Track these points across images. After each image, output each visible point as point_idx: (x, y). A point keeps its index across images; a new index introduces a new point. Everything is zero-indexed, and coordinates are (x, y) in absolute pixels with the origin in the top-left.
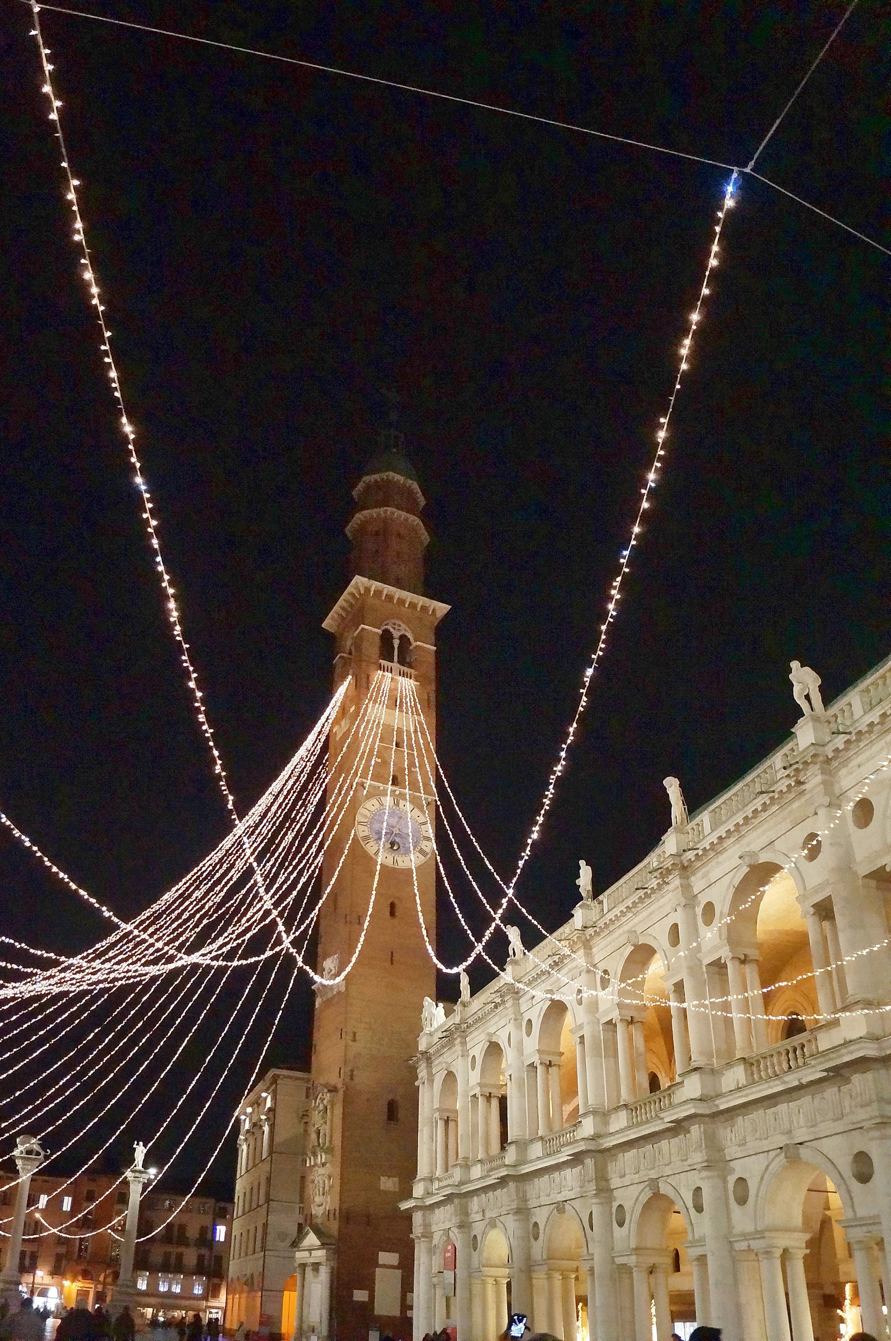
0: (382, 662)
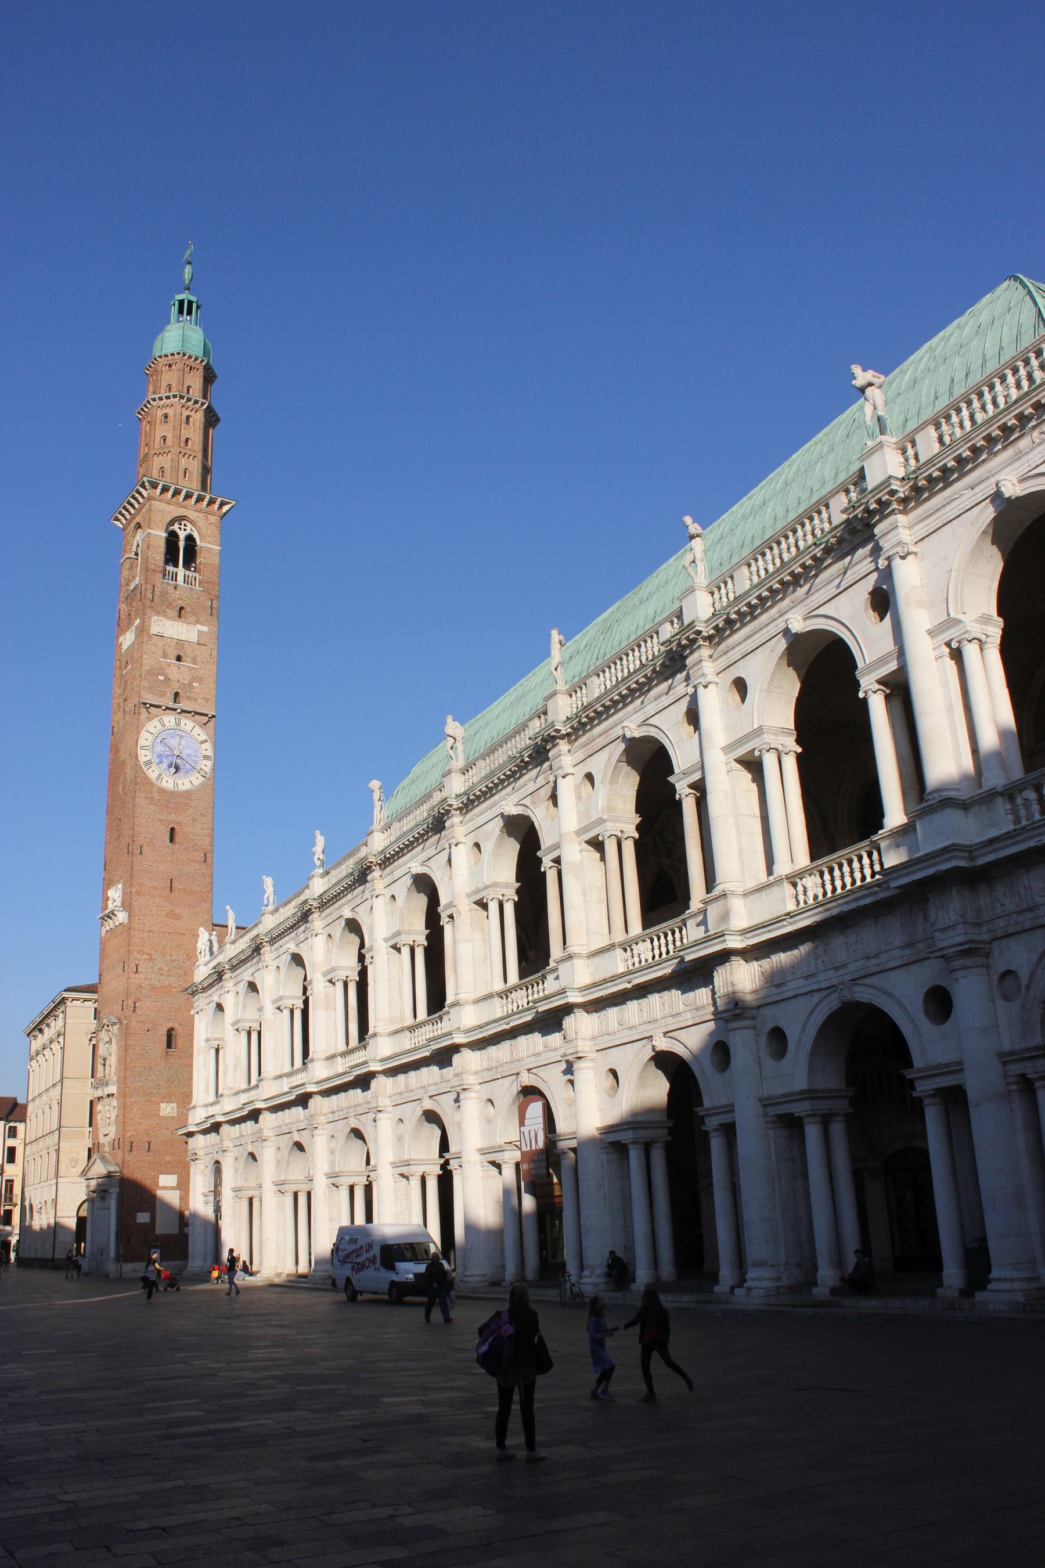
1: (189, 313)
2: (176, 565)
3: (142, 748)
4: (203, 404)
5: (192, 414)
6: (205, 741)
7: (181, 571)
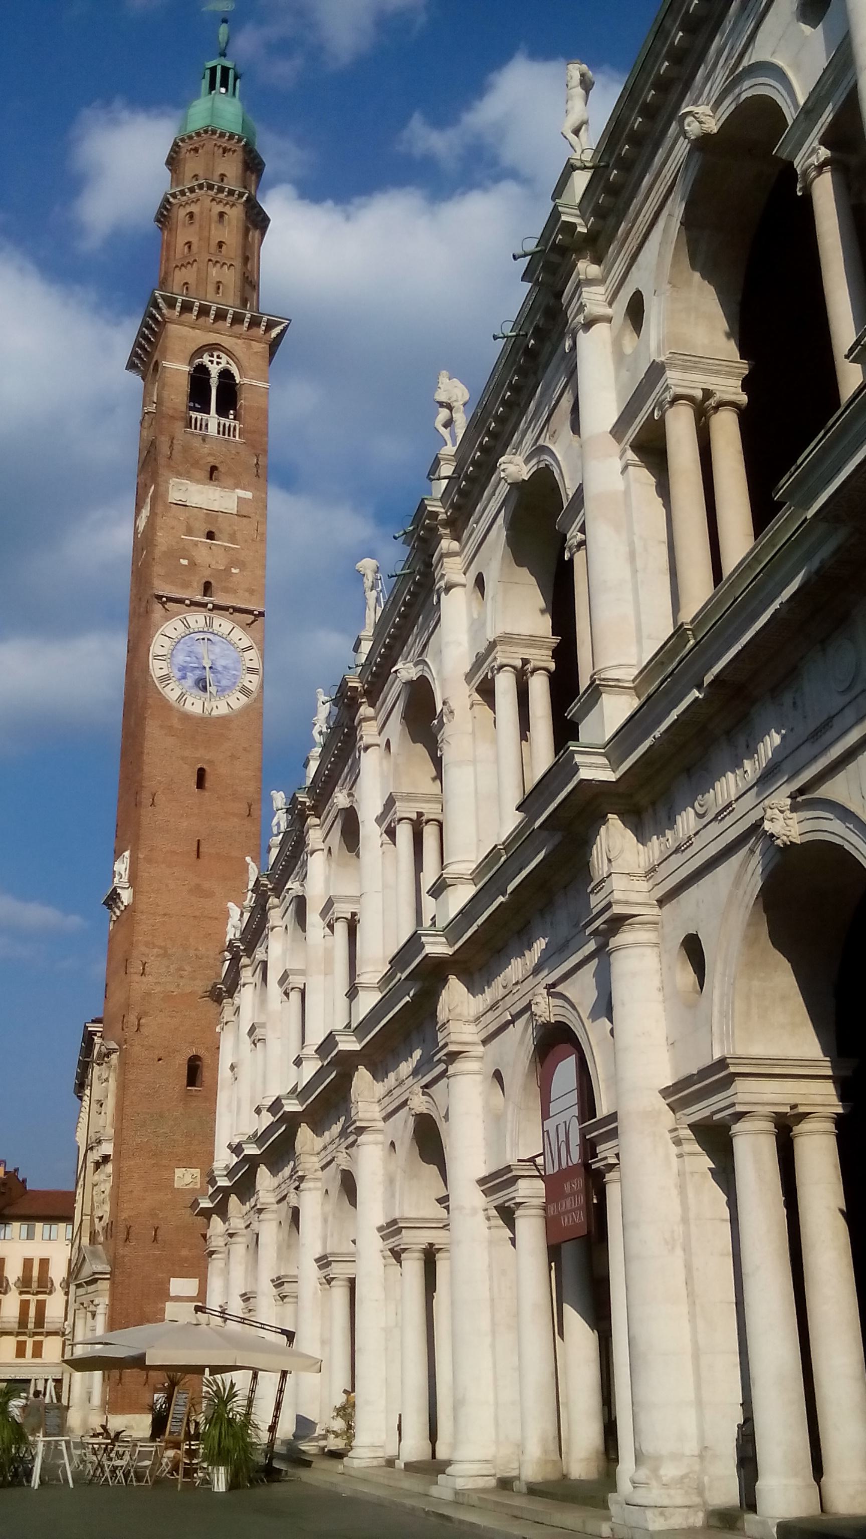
0: (194, 415)
1: (224, 84)
2: (208, 412)
3: (156, 657)
4: (241, 195)
5: (227, 209)
6: (250, 648)
7: (213, 420)
